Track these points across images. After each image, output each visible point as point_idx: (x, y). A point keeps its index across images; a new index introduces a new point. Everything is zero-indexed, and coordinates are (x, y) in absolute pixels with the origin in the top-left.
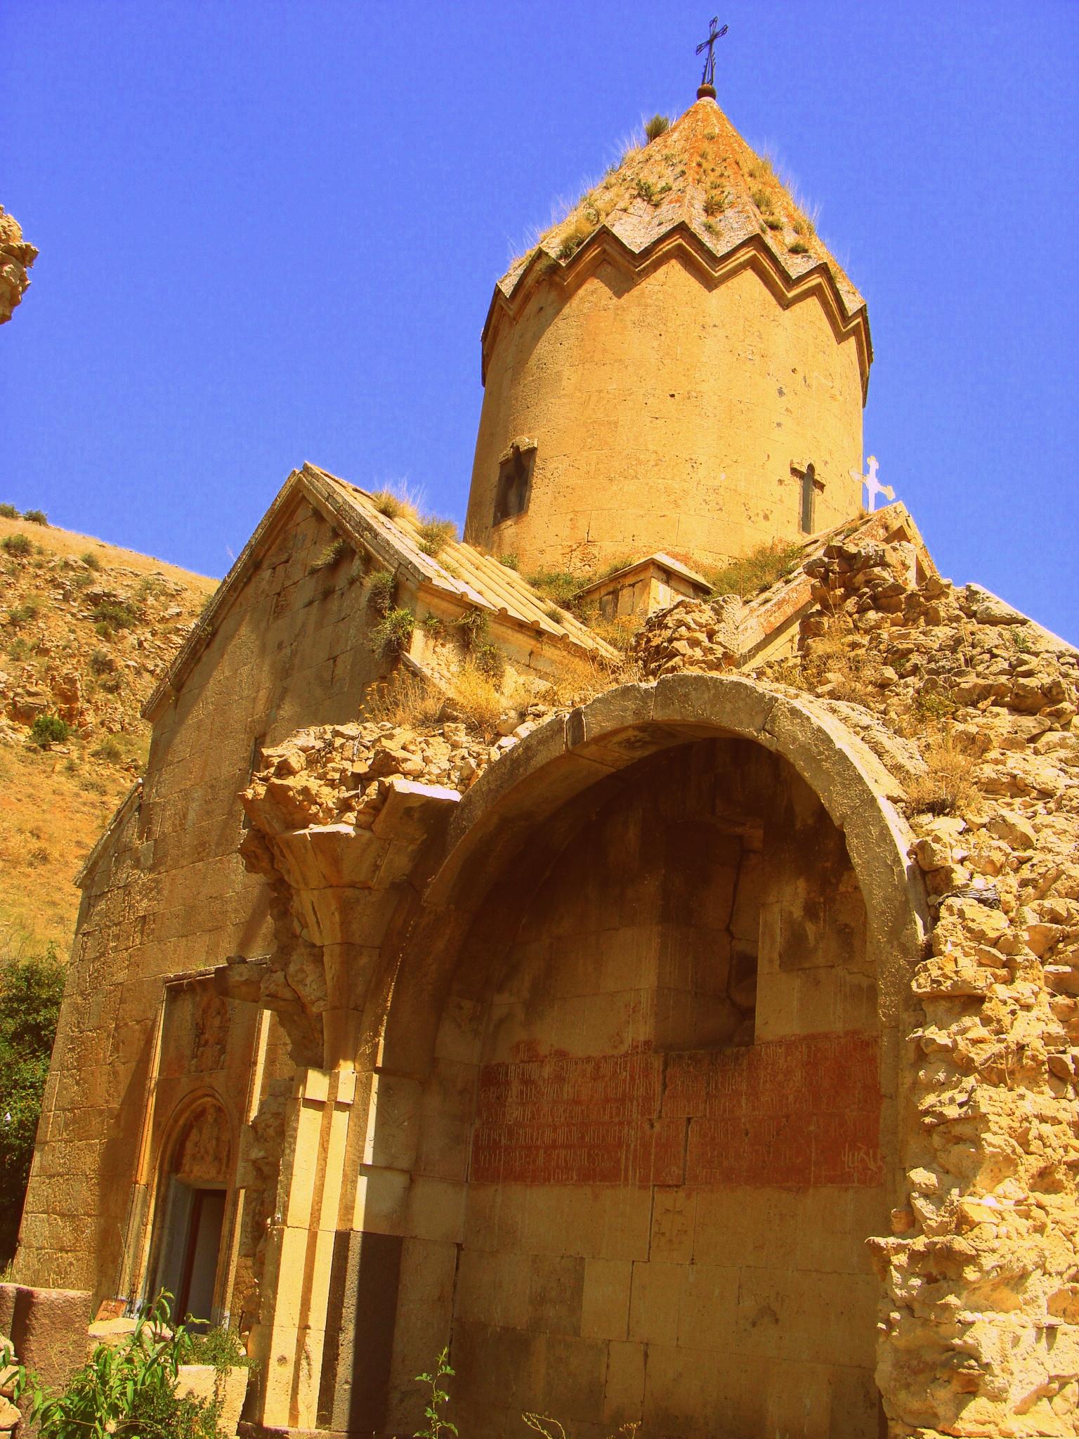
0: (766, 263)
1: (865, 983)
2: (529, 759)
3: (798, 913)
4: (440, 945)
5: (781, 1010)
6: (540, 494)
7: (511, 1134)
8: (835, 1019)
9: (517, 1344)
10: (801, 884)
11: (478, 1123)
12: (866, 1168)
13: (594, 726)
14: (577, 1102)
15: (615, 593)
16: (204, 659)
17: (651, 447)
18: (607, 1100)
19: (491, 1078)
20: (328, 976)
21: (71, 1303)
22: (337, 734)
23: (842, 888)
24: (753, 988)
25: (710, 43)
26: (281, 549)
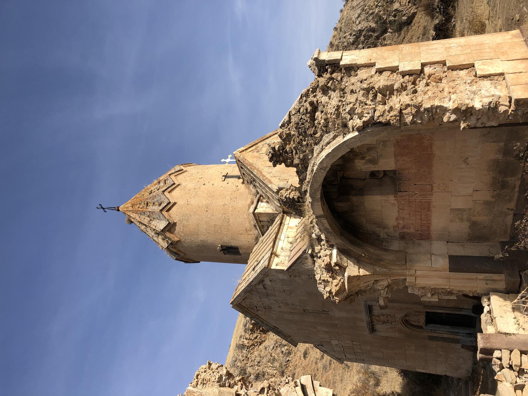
0: (170, 189)
1: (382, 143)
2: (327, 229)
3: (363, 161)
4: (372, 250)
5: (387, 164)
6: (233, 243)
7: (418, 231)
8: (391, 149)
9: (474, 224)
10: (356, 161)
11: (414, 240)
12: (429, 139)
13: (321, 213)
14: (410, 213)
15: (260, 221)
16: (281, 329)
17: (221, 216)
18: (409, 206)
19: (403, 237)
20: (382, 278)
21: (482, 338)
22: (320, 280)
23: (358, 151)
24: (378, 171)
25: (104, 209)
26: (253, 309)
